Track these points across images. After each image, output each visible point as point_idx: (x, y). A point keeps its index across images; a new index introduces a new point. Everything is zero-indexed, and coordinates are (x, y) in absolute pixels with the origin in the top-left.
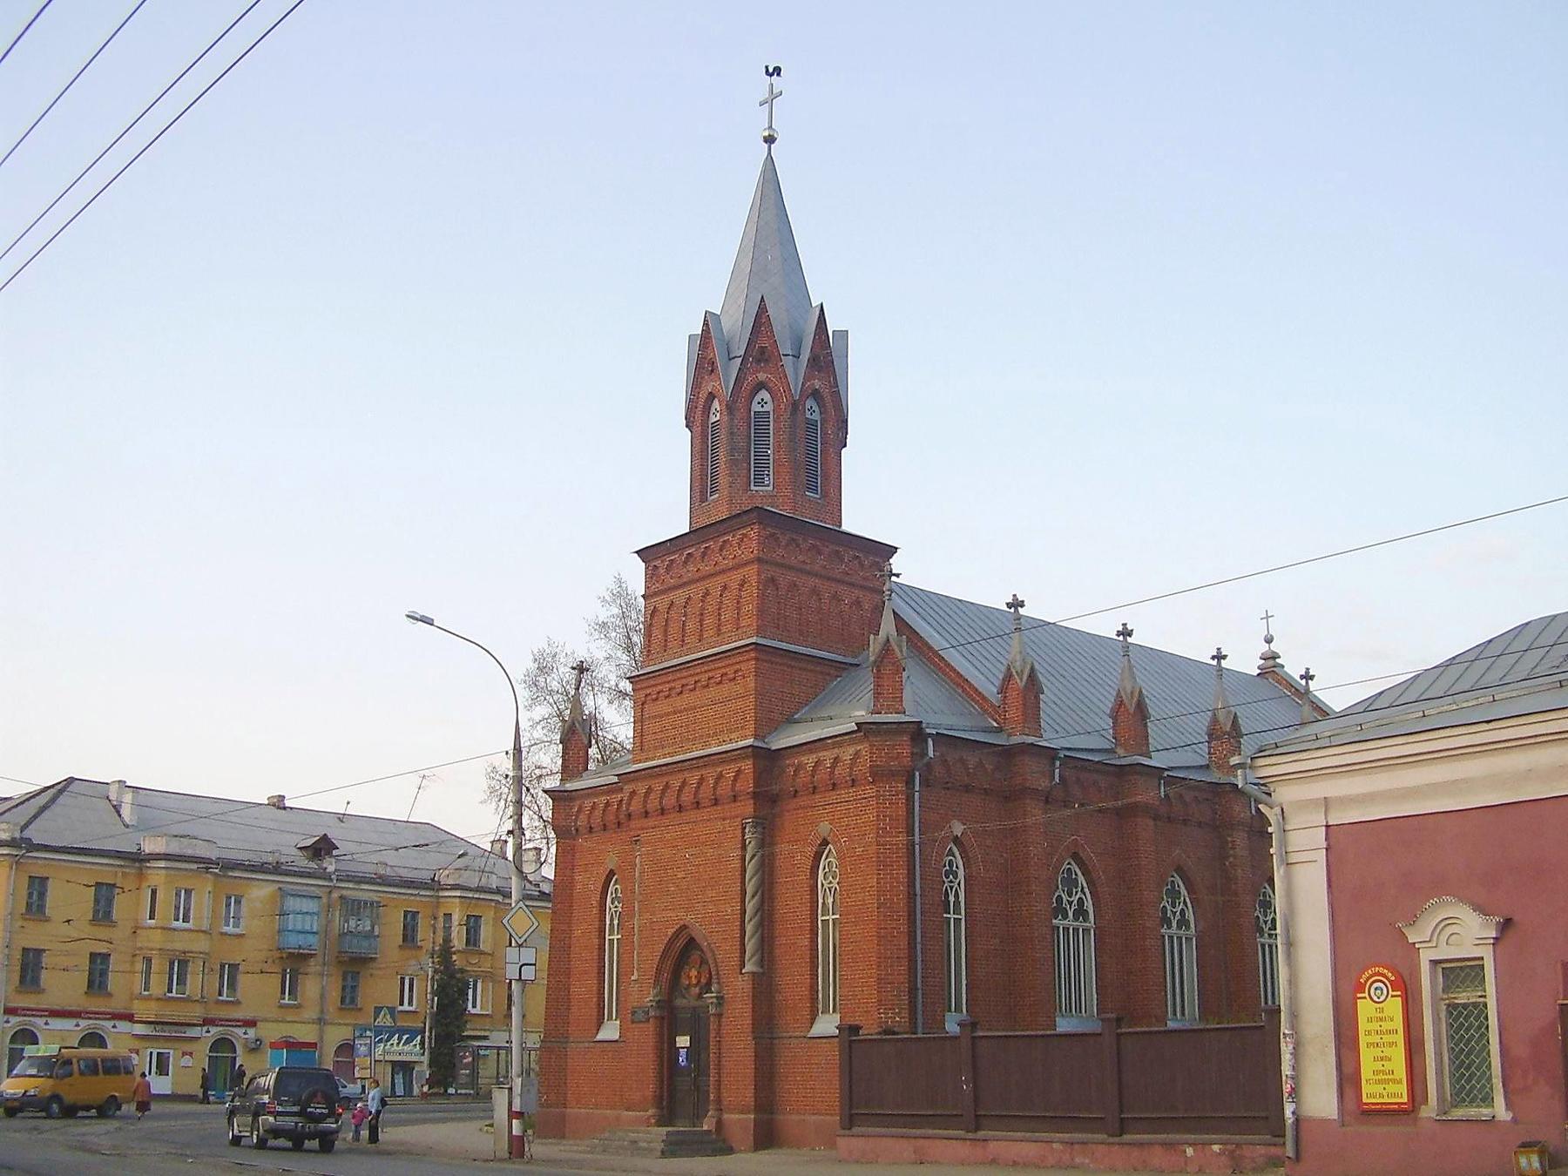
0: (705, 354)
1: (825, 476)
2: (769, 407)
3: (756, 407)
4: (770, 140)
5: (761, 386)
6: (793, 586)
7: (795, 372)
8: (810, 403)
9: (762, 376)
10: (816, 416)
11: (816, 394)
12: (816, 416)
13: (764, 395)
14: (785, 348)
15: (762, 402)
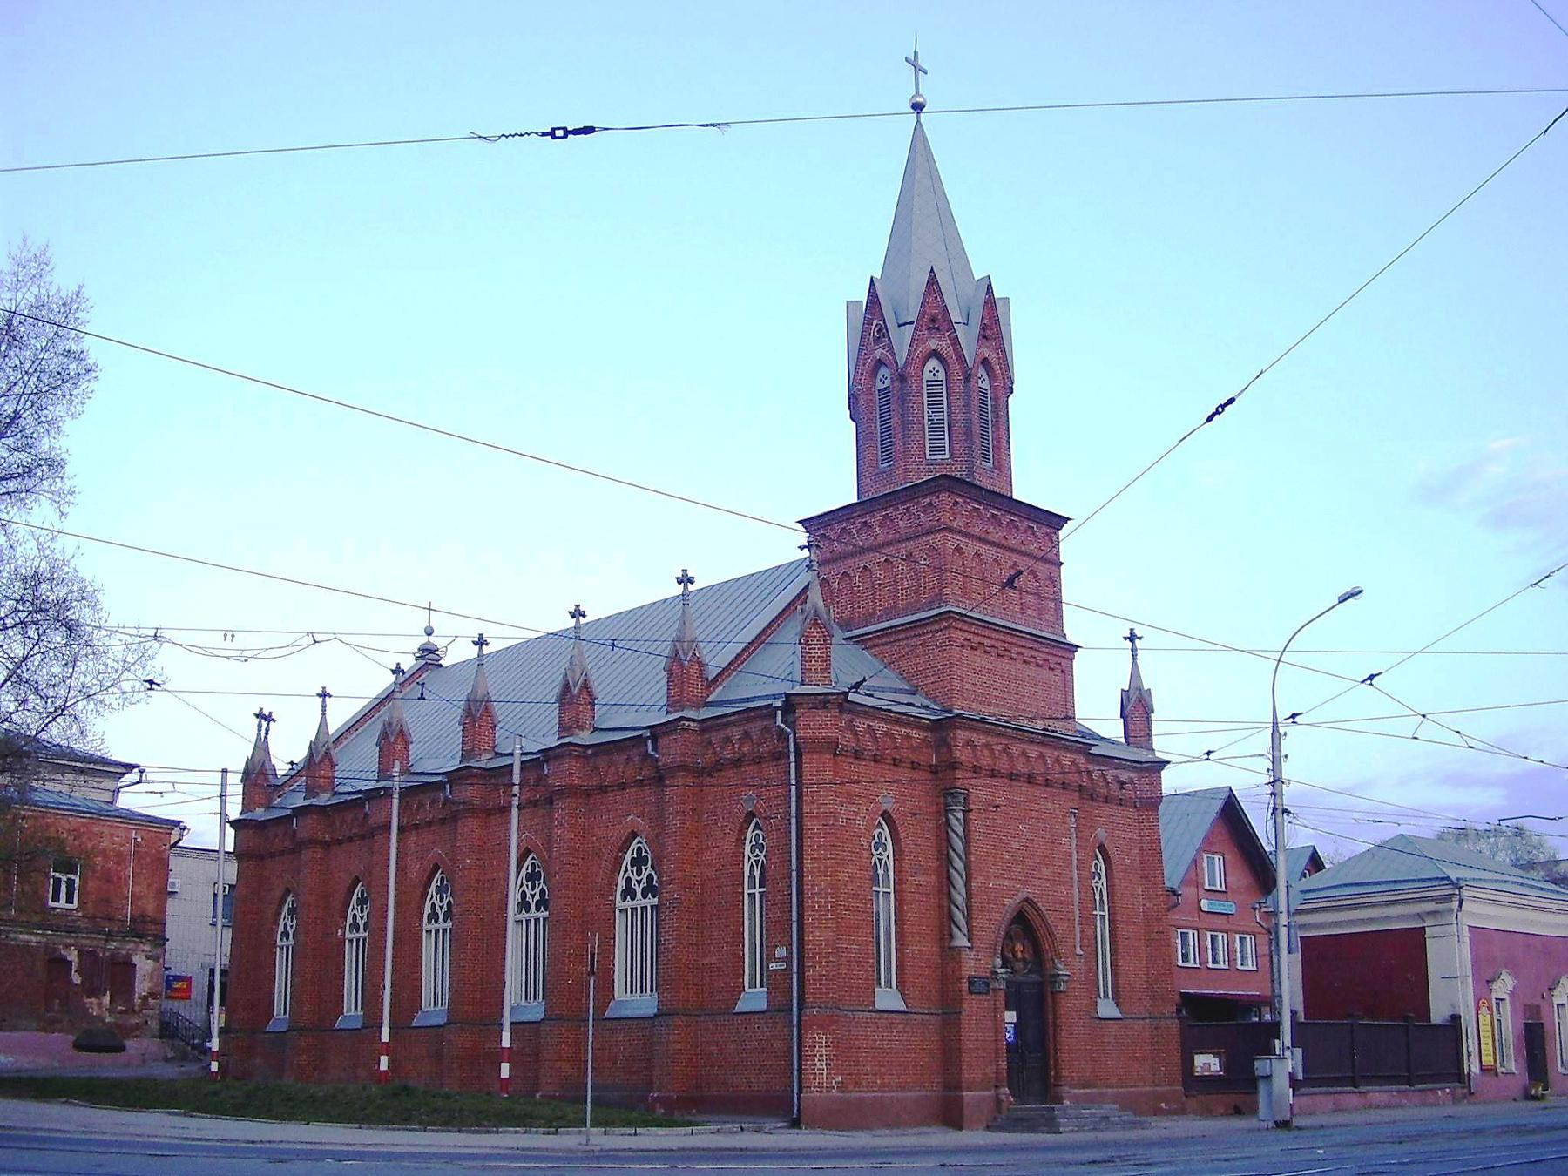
0: (871, 321)
1: (997, 448)
2: (941, 376)
3: (927, 376)
4: (918, 107)
5: (935, 354)
6: (978, 554)
7: (968, 338)
8: (982, 371)
9: (933, 344)
10: (986, 385)
11: (985, 362)
12: (986, 385)
13: (933, 363)
14: (956, 317)
15: (934, 372)
